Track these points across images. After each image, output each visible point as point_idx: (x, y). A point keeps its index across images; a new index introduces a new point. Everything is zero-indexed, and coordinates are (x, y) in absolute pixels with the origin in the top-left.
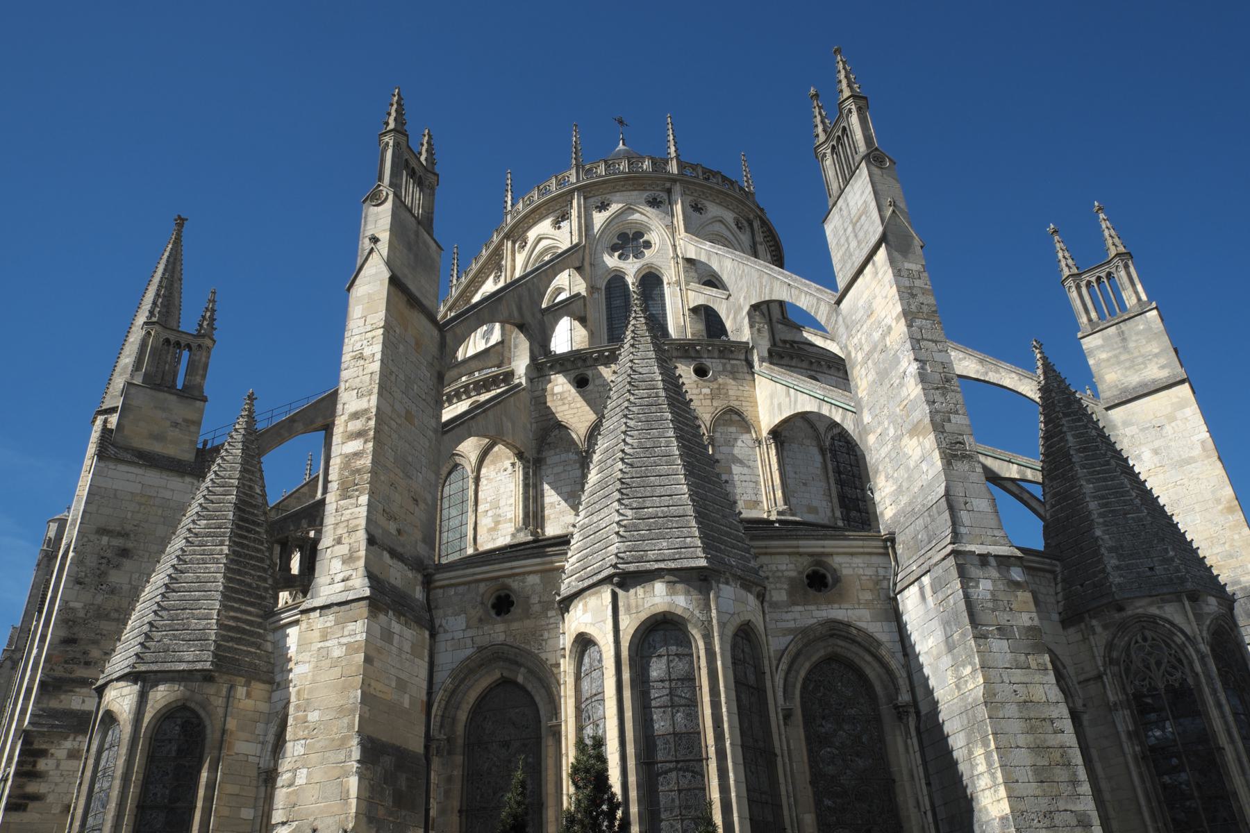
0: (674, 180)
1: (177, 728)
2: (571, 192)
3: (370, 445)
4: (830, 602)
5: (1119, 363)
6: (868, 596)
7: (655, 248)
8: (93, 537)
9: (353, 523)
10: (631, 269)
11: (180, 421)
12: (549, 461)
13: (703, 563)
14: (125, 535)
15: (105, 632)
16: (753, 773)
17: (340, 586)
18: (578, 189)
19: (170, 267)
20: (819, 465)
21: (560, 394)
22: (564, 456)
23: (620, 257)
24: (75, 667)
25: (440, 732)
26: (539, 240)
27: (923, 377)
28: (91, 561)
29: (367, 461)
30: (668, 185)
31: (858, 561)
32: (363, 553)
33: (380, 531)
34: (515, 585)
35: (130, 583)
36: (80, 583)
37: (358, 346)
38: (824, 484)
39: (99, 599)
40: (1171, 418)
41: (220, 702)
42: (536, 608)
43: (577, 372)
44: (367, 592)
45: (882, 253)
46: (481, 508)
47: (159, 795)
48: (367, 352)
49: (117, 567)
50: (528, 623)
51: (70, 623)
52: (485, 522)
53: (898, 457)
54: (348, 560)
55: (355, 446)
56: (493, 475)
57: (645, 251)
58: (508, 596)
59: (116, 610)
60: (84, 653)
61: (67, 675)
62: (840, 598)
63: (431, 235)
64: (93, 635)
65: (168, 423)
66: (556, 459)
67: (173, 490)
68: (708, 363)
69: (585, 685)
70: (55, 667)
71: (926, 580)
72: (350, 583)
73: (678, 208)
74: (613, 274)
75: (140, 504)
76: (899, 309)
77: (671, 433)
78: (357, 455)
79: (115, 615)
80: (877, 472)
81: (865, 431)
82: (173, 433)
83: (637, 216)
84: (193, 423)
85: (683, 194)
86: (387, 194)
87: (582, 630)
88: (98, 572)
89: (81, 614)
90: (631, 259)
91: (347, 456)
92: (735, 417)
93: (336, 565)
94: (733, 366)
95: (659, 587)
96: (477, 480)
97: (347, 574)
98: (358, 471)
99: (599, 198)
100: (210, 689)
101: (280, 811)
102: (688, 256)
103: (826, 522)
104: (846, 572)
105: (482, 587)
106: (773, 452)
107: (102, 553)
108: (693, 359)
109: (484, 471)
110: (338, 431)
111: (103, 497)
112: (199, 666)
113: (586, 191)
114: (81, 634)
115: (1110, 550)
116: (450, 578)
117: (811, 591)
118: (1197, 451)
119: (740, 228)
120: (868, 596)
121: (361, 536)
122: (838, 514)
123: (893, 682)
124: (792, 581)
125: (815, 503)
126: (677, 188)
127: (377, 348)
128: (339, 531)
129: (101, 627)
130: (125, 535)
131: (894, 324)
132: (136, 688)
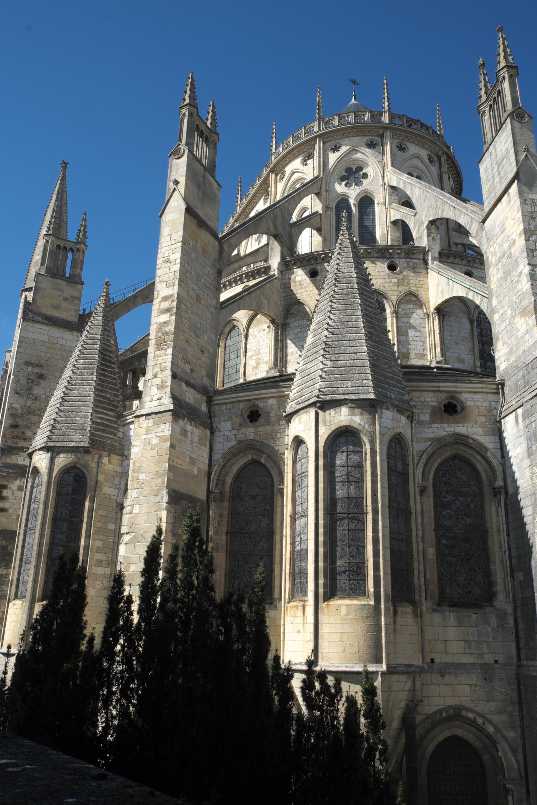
0: (385, 128)
1: (71, 478)
2: (315, 138)
3: (174, 317)
4: (457, 422)
6: (483, 419)
7: (370, 178)
8: (24, 367)
9: (164, 365)
11: (68, 297)
12: (291, 325)
13: (372, 396)
15: (33, 422)
16: (395, 523)
17: (157, 403)
18: (319, 136)
19: (60, 196)
20: (468, 331)
21: (300, 281)
22: (300, 322)
23: (346, 185)
24: (19, 441)
25: (216, 488)
26: (293, 173)
28: (23, 381)
29: (171, 328)
30: (381, 131)
31: (478, 397)
32: (169, 383)
33: (180, 370)
34: (261, 404)
35: (45, 394)
36: (18, 393)
37: (166, 254)
38: (470, 344)
39: (29, 403)
41: (93, 465)
42: (274, 419)
43: (311, 267)
44: (171, 407)
46: (248, 354)
47: (64, 513)
48: (172, 258)
49: (38, 384)
50: (268, 428)
51: (14, 416)
52: (251, 363)
53: (511, 329)
54: (161, 387)
55: (165, 317)
56: (256, 333)
57: (364, 181)
58: (257, 411)
59: (38, 410)
60: (23, 433)
61: (14, 445)
62: (464, 420)
63: (213, 177)
64: (27, 423)
65: (62, 299)
66: (296, 324)
67: (66, 340)
68: (397, 261)
69: (299, 466)
70: (8, 440)
71: (520, 411)
72: (162, 401)
73: (388, 148)
74: (341, 198)
75: (48, 348)
76: (522, 228)
77: (359, 313)
78: (166, 323)
79: (37, 412)
80: (498, 339)
81: (493, 311)
82: (65, 305)
83: (359, 155)
84: (76, 298)
85: (392, 138)
86: (184, 151)
87: (298, 434)
88: (28, 387)
89: (20, 411)
90: (354, 186)
91: (160, 324)
92: (413, 298)
93: (154, 390)
94: (414, 263)
95: (344, 410)
96: (247, 336)
97: (160, 396)
98: (167, 333)
99: (333, 142)
100: (88, 458)
101: (125, 527)
102: (392, 185)
103: (469, 369)
104: (469, 403)
105: (242, 405)
106: (436, 322)
107: (28, 376)
108: (387, 258)
109: (251, 331)
111: (27, 343)
112: (82, 445)
113: (324, 137)
114: (20, 422)
116: (223, 399)
117: (446, 415)
119: (431, 162)
120: (483, 419)
121: (168, 373)
122: (478, 363)
123: (493, 473)
124: (433, 408)
125: (463, 356)
126: (388, 134)
127: (178, 256)
128: (156, 370)
129: (31, 419)
131: (517, 239)
132: (49, 455)
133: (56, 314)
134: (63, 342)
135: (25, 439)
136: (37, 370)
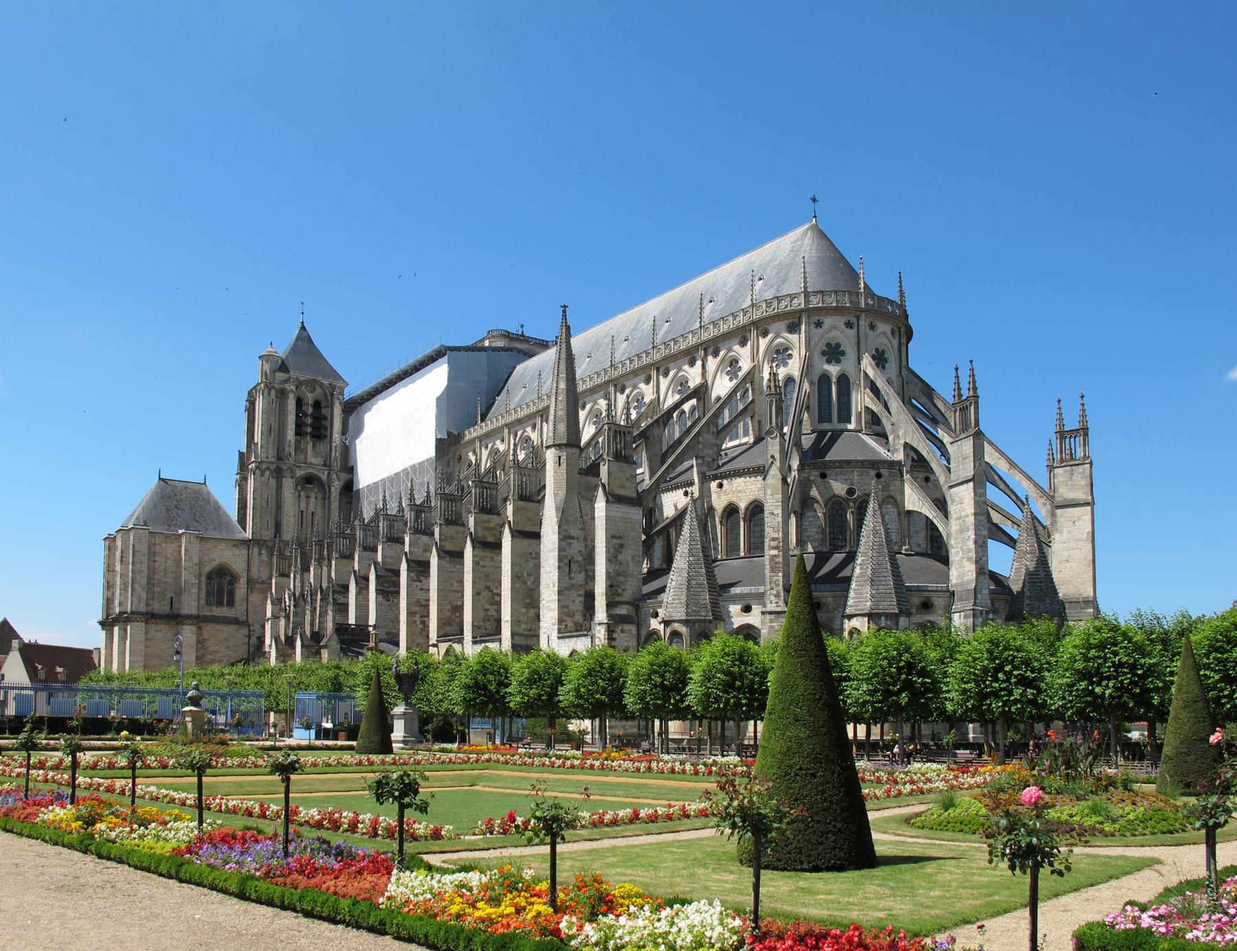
0: (862, 311)
5: (1067, 485)
10: (833, 370)
14: (620, 538)
27: (976, 542)
28: (612, 552)
30: (858, 313)
40: (1079, 519)
45: (971, 484)
48: (775, 512)
54: (777, 596)
55: (774, 552)
62: (933, 612)
76: (973, 511)
108: (876, 469)
110: (766, 548)
114: (615, 584)
115: (1028, 597)
118: (1085, 536)
119: (893, 334)
121: (781, 588)
124: (917, 606)
130: (620, 538)
133: (622, 492)
134: (630, 516)
135: (618, 595)
136: (619, 541)
